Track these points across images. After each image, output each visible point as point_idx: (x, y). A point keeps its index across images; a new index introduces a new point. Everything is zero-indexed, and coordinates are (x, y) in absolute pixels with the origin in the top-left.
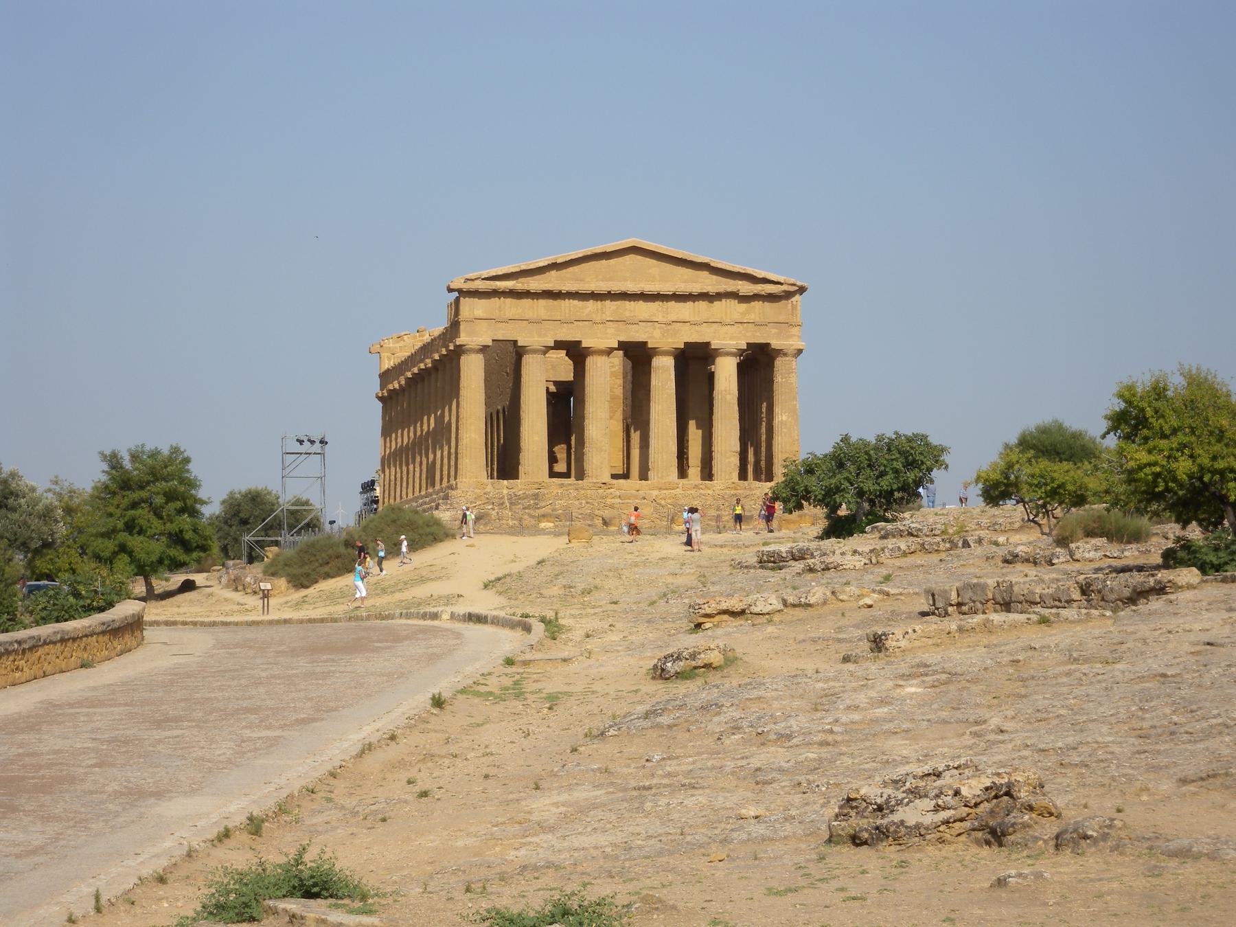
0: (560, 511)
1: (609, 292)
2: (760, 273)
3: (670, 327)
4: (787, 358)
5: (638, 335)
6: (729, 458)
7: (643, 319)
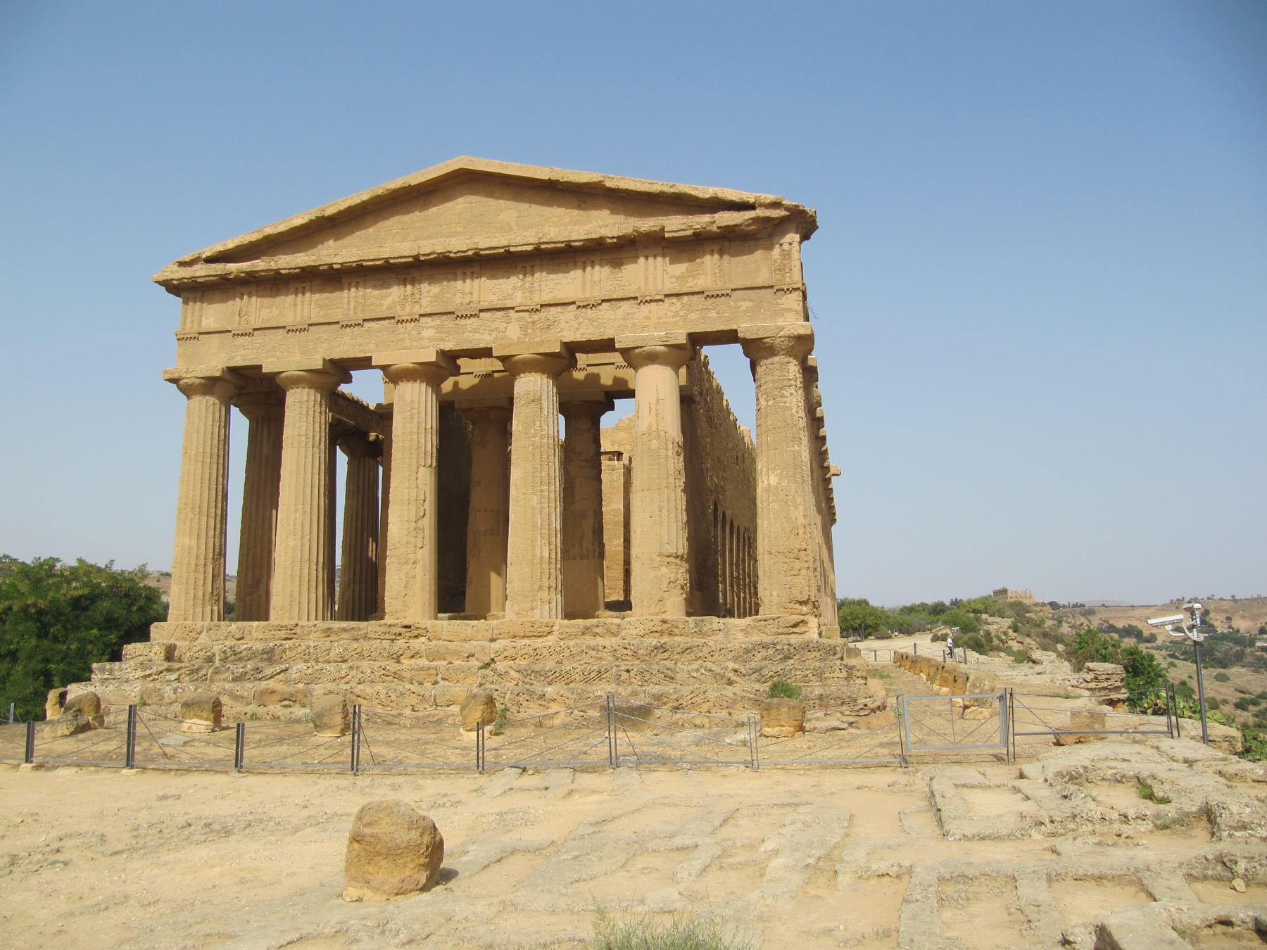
0: (301, 686)
1: (416, 258)
2: (704, 191)
3: (536, 317)
4: (777, 359)
5: (478, 336)
6: (658, 568)
7: (485, 305)
